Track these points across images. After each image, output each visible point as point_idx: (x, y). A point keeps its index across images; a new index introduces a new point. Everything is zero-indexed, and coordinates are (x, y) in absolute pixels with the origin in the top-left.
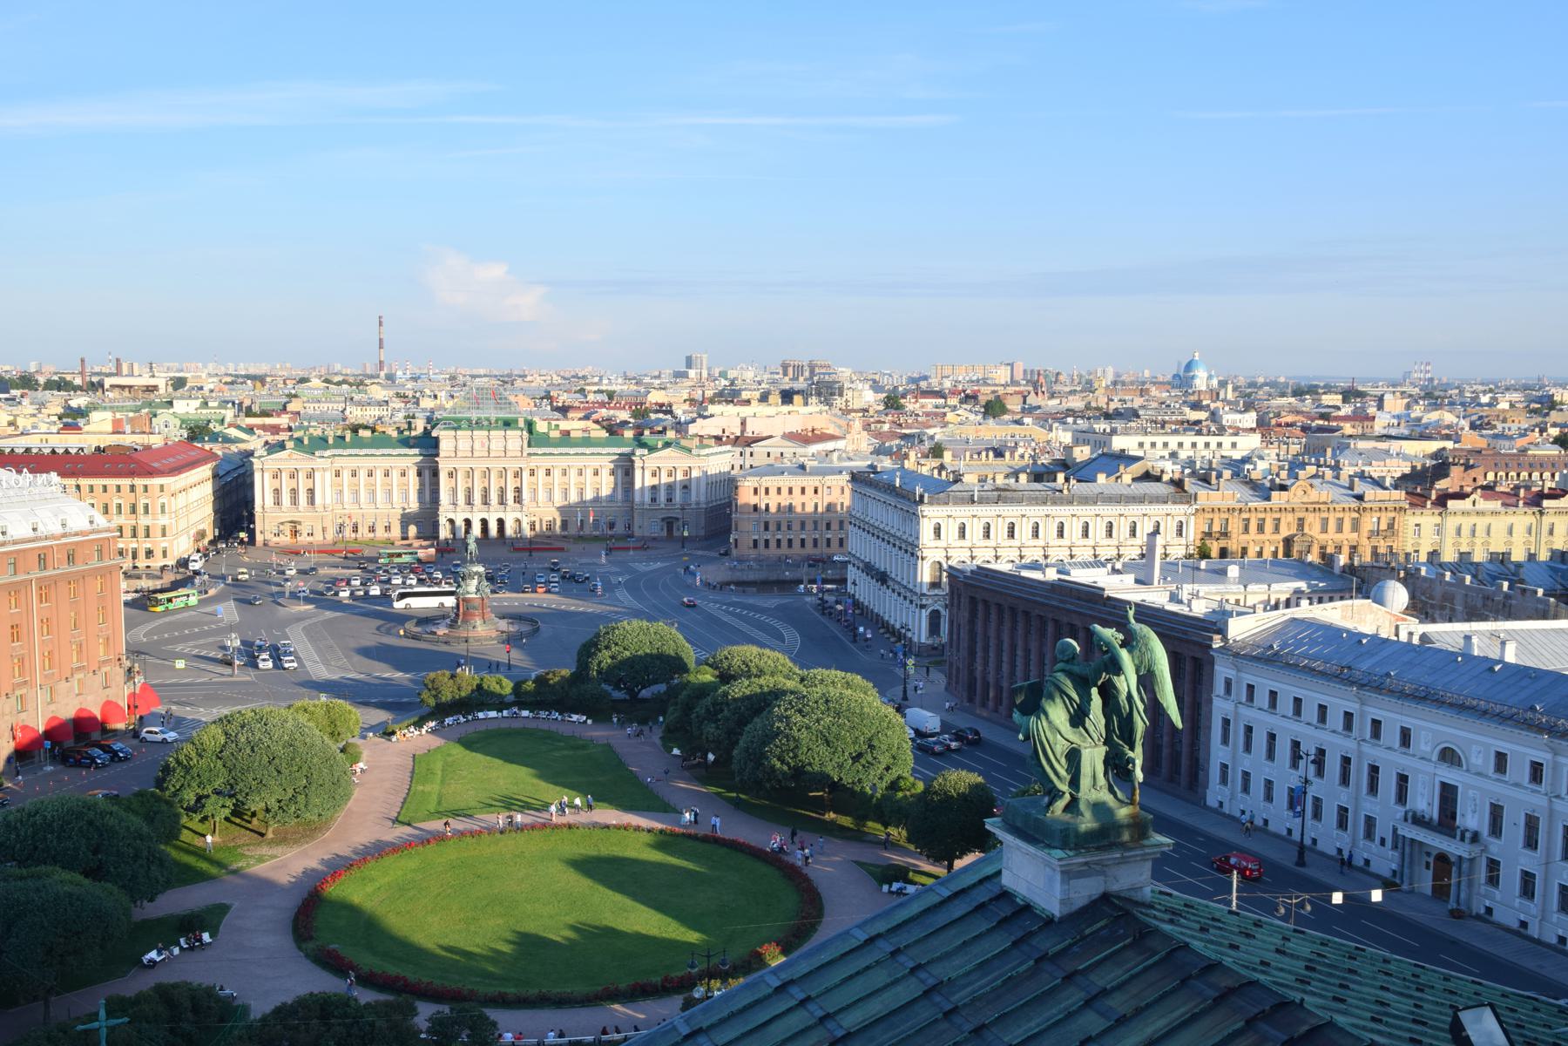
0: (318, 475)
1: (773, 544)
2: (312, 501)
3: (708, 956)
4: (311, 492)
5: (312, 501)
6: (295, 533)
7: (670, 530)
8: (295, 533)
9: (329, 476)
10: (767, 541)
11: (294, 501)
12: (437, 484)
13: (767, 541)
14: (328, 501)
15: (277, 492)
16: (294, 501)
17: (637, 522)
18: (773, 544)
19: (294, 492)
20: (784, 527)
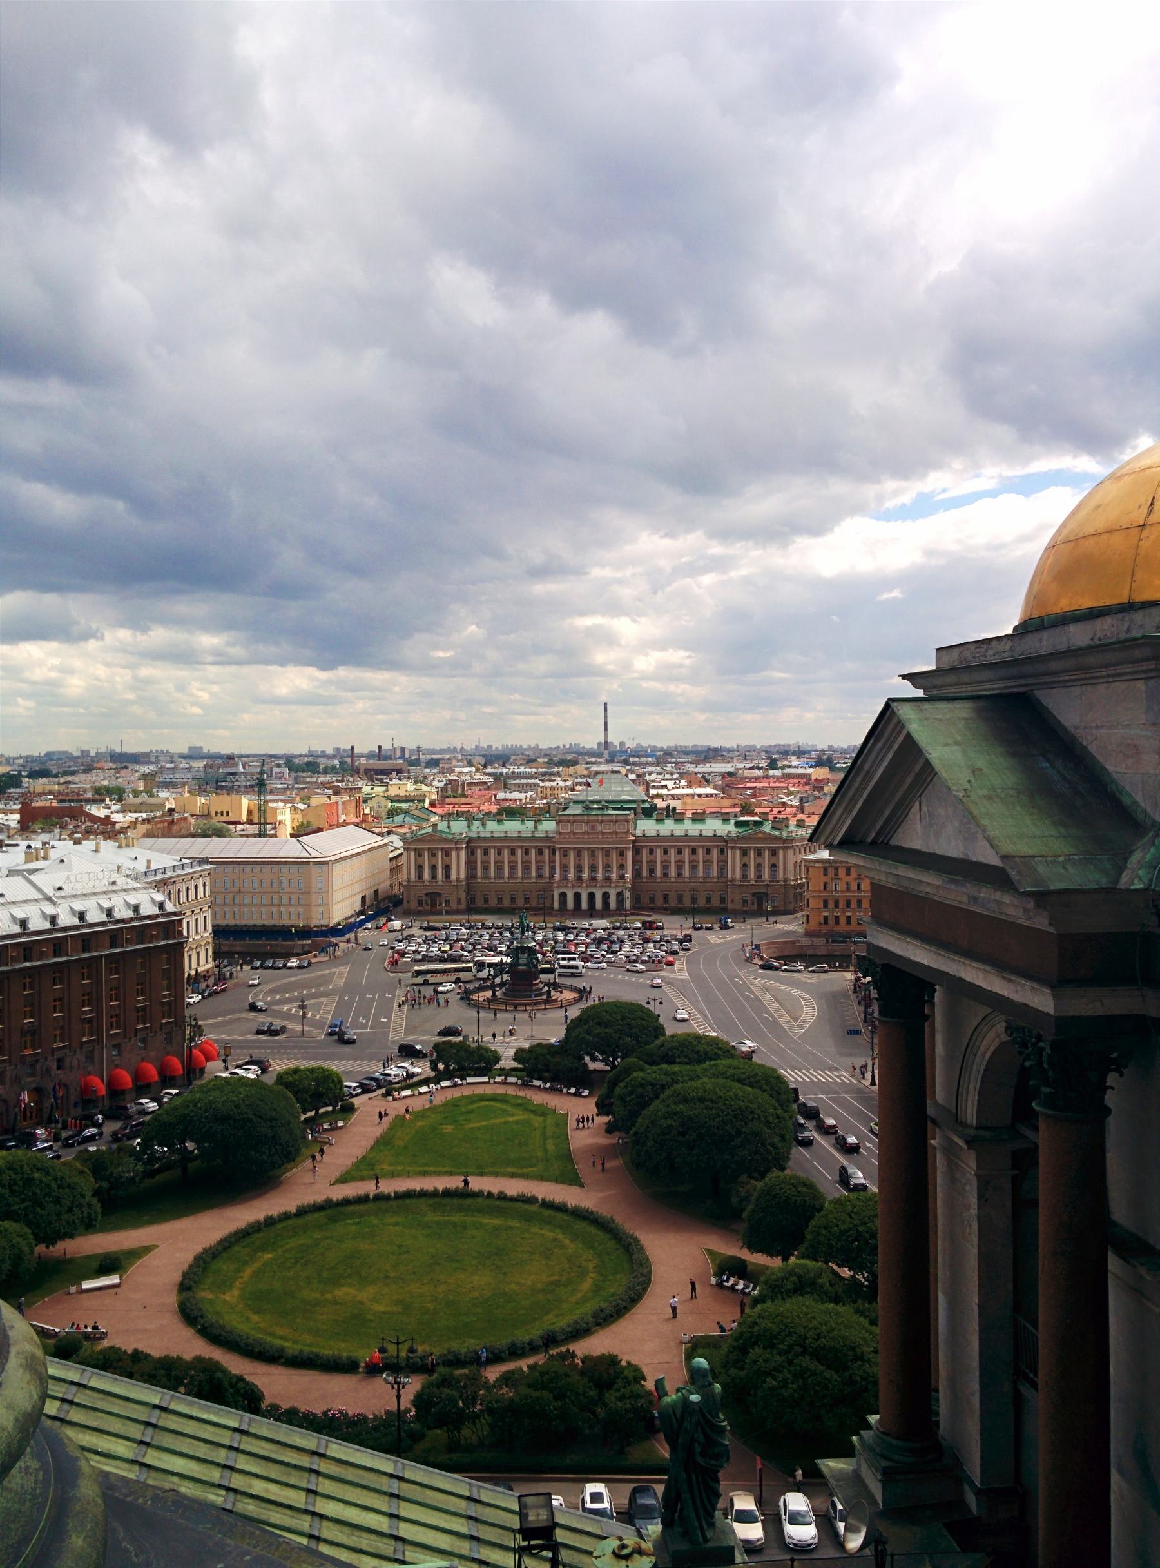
0: (454, 854)
1: (843, 921)
2: (447, 876)
3: (398, 1343)
4: (447, 868)
5: (447, 876)
6: (434, 905)
7: (760, 904)
8: (434, 905)
9: (463, 854)
10: (837, 918)
11: (434, 876)
12: (554, 861)
13: (837, 918)
14: (463, 876)
15: (420, 868)
16: (434, 876)
17: (729, 896)
18: (843, 921)
19: (433, 868)
20: (854, 905)
